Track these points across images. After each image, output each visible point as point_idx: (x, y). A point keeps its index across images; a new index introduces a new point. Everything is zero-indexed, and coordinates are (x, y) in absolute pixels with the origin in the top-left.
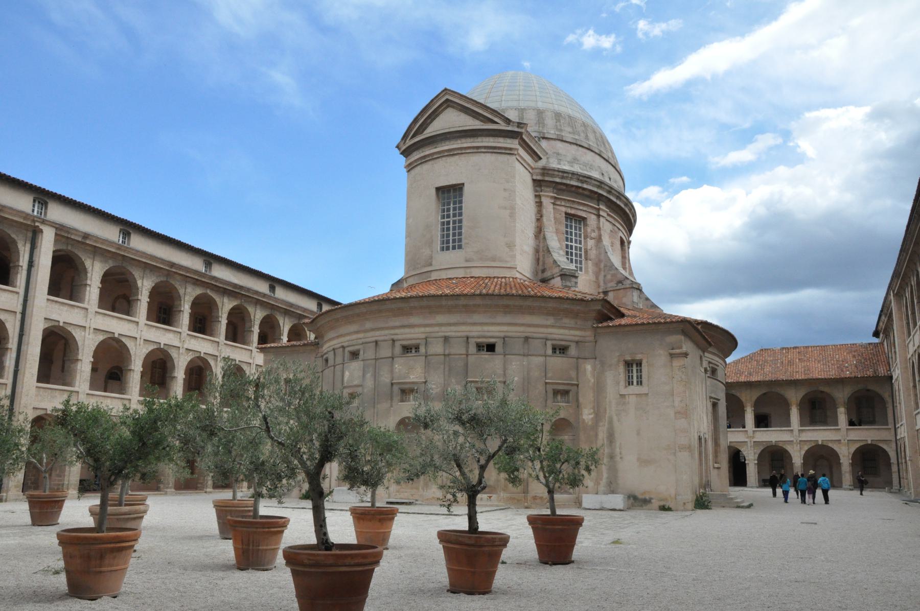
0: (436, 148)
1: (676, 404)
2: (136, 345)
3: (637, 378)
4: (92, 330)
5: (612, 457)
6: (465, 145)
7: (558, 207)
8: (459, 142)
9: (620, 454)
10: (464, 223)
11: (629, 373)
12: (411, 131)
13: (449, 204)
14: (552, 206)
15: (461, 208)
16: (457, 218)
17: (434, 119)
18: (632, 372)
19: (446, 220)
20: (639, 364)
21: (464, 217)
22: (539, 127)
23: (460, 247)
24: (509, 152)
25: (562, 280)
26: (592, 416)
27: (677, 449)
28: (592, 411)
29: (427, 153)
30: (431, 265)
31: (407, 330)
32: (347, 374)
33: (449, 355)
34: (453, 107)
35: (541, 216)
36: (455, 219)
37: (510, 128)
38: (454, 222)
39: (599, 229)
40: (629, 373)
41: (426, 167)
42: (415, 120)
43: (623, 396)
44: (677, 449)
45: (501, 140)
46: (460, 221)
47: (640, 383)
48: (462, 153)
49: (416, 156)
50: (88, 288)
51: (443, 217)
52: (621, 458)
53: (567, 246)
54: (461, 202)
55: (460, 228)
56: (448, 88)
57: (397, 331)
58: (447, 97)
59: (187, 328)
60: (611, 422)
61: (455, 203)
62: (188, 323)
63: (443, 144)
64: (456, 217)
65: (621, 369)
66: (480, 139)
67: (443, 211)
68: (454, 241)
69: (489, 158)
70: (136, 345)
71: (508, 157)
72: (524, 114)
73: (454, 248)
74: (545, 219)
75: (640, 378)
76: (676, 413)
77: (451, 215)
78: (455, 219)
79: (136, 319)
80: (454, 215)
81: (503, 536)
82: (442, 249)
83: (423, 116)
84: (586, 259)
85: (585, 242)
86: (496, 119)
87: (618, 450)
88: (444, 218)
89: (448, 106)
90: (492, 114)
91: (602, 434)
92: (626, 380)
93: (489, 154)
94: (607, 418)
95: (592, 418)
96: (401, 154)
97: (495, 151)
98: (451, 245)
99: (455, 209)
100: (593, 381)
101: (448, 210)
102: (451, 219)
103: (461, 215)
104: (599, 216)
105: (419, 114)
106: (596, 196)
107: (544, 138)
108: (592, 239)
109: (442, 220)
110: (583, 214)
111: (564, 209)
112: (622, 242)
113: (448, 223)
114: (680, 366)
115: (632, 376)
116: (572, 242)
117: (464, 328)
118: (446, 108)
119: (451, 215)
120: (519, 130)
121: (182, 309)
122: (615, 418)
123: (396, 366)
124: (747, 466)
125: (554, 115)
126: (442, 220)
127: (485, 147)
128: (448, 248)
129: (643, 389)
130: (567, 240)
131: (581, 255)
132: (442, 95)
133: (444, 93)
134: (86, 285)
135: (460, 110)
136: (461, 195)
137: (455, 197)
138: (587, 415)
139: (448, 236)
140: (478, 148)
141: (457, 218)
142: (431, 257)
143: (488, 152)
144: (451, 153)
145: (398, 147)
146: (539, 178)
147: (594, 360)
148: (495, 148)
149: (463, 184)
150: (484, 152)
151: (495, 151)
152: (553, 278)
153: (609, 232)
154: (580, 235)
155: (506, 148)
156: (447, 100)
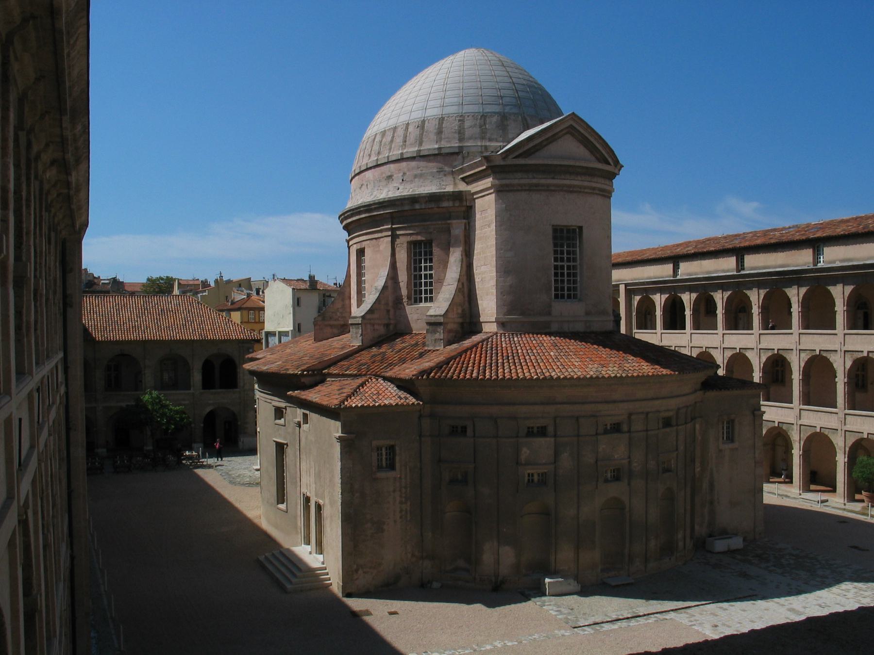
0: (553, 178)
1: (757, 455)
5: (712, 503)
6: (586, 184)
8: (579, 178)
17: (551, 142)
19: (559, 264)
23: (575, 296)
29: (543, 181)
30: (549, 313)
34: (573, 135)
36: (568, 264)
38: (569, 268)
43: (721, 451)
48: (580, 192)
51: (556, 260)
56: (576, 112)
63: (563, 177)
64: (570, 262)
66: (595, 179)
67: (556, 252)
73: (569, 297)
77: (565, 258)
78: (568, 264)
80: (569, 260)
82: (556, 296)
86: (610, 160)
88: (573, 266)
90: (608, 153)
99: (568, 253)
100: (700, 438)
102: (565, 264)
109: (556, 263)
113: (562, 267)
119: (565, 258)
126: (556, 263)
128: (563, 297)
129: (736, 445)
140: (594, 189)
143: (599, 194)
144: (571, 190)
149: (581, 228)
150: (597, 194)
156: (571, 125)
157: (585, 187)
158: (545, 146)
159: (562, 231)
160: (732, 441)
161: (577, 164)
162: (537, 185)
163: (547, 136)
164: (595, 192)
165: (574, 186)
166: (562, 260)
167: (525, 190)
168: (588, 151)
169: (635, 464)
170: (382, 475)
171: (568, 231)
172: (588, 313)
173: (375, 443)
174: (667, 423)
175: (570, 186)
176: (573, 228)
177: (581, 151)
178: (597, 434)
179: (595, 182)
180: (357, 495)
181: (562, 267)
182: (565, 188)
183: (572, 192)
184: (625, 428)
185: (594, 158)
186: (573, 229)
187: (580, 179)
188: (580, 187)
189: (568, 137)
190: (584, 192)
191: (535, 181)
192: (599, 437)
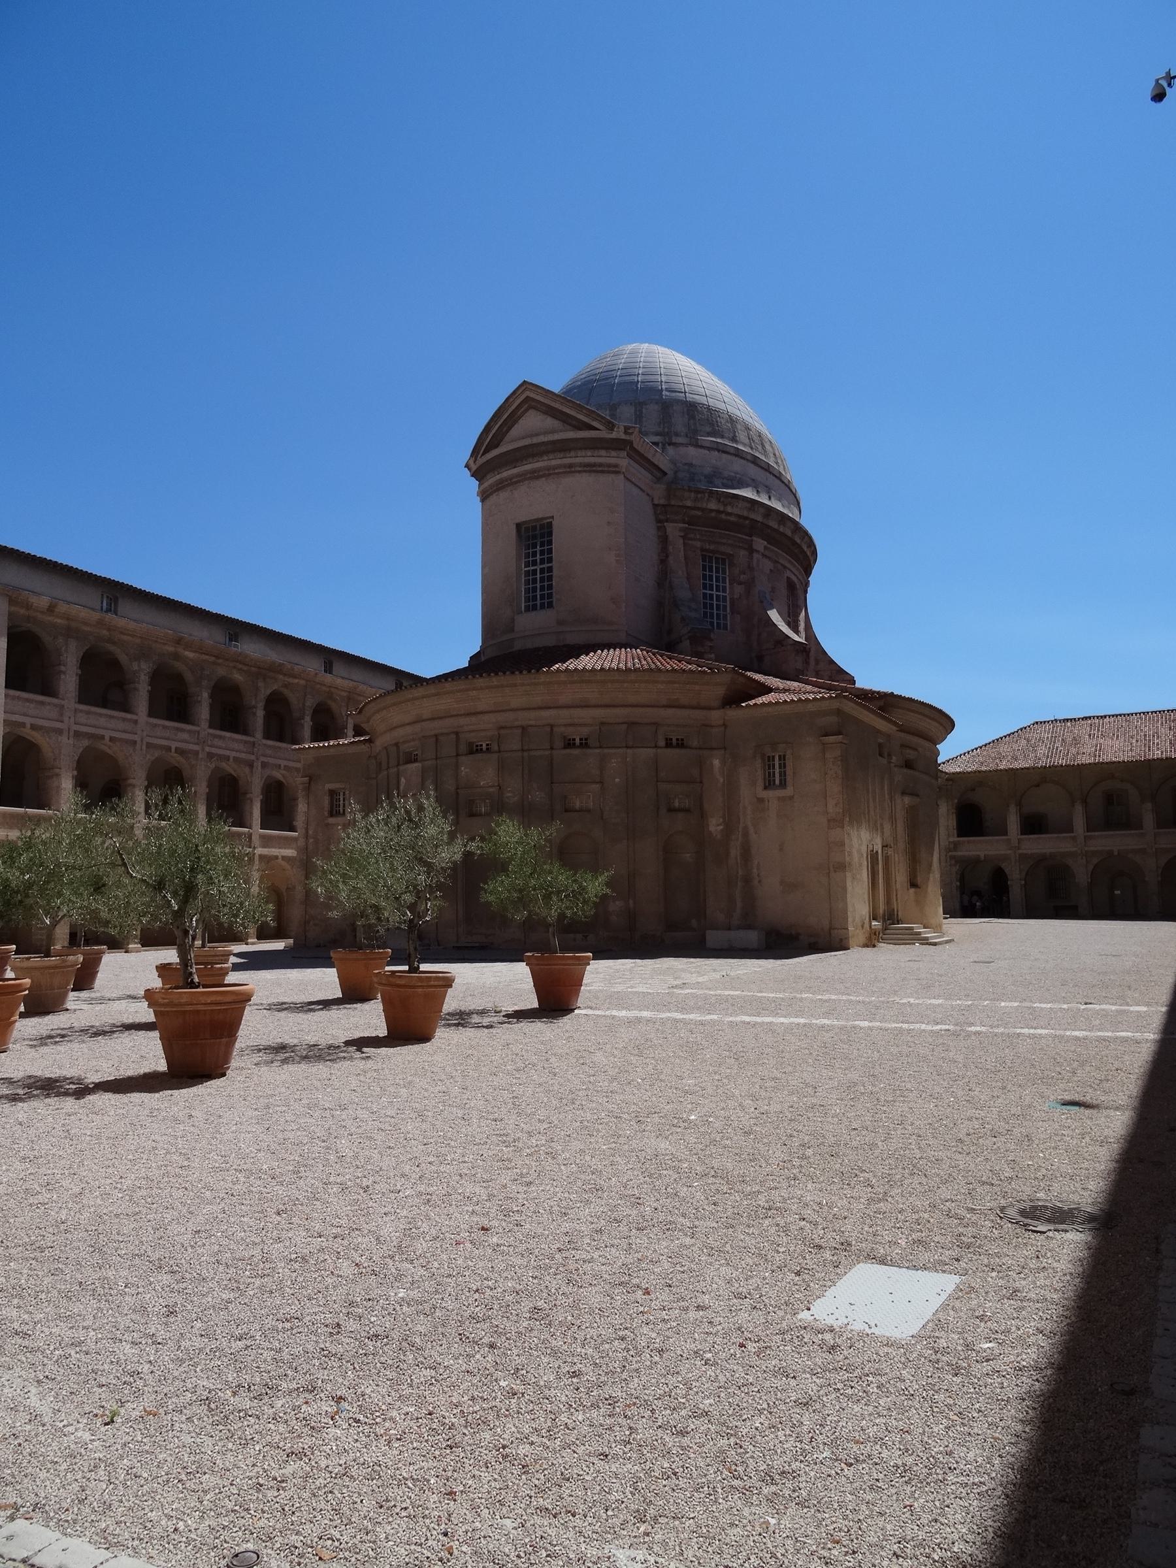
1: (831, 809)
2: (134, 750)
3: (780, 776)
4: (72, 733)
5: (747, 880)
6: (554, 463)
7: (690, 542)
9: (758, 875)
10: (555, 572)
11: (769, 768)
12: (483, 443)
13: (534, 546)
14: (681, 541)
15: (550, 551)
16: (546, 566)
18: (774, 768)
20: (783, 758)
21: (555, 564)
22: (664, 428)
23: (550, 605)
24: (613, 470)
25: (691, 644)
26: (721, 827)
27: (831, 869)
28: (721, 820)
30: (512, 630)
31: (474, 719)
32: (403, 780)
33: (529, 750)
35: (667, 556)
36: (542, 566)
37: (614, 435)
39: (751, 568)
40: (769, 768)
41: (503, 495)
42: (487, 428)
43: (761, 800)
44: (831, 869)
45: (603, 453)
46: (550, 569)
47: (783, 785)
48: (550, 475)
49: (491, 480)
50: (63, 677)
52: (760, 881)
53: (705, 594)
54: (550, 542)
55: (550, 578)
57: (463, 721)
58: (528, 393)
59: (207, 724)
60: (746, 834)
61: (542, 545)
62: (208, 717)
65: (758, 763)
66: (573, 454)
67: (527, 556)
68: (542, 597)
69: (586, 479)
70: (134, 750)
71: (613, 476)
72: (644, 410)
73: (542, 606)
74: (671, 558)
75: (783, 774)
76: (829, 821)
77: (538, 561)
78: (542, 566)
79: (134, 717)
81: (449, 975)
83: (496, 423)
84: (732, 612)
85: (730, 588)
86: (595, 424)
87: (755, 870)
89: (530, 407)
90: (588, 416)
91: (735, 852)
92: (765, 779)
93: (587, 474)
94: (740, 829)
95: (722, 830)
96: (472, 476)
97: (594, 469)
98: (538, 602)
99: (542, 552)
100: (722, 780)
101: (534, 554)
102: (538, 568)
103: (550, 560)
104: (751, 550)
105: (492, 419)
106: (747, 522)
107: (670, 444)
108: (740, 583)
110: (729, 551)
111: (698, 544)
112: (791, 586)
113: (534, 572)
114: (835, 758)
115: (774, 773)
116: (713, 590)
117: (546, 714)
118: (526, 410)
119: (538, 561)
120: (627, 437)
121: (199, 698)
122: (751, 830)
123: (463, 768)
124: (1010, 889)
125: (685, 410)
127: (581, 465)
128: (534, 608)
129: (788, 791)
130: (705, 587)
131: (725, 607)
132: (521, 391)
133: (523, 388)
134: (61, 672)
135: (545, 413)
136: (550, 534)
137: (542, 536)
138: (715, 826)
139: (534, 590)
140: (571, 466)
141: (546, 566)
142: (513, 620)
143: (585, 471)
144: (535, 475)
145: (467, 466)
146: (662, 502)
147: (723, 752)
148: (594, 465)
150: (579, 472)
151: (594, 469)
152: (681, 642)
153: (768, 572)
154: (724, 579)
155: (609, 466)
156: (527, 397)
157: (555, 468)
158: (507, 432)
159: (534, 528)
160: (783, 785)
161: (535, 440)
162: (501, 481)
163: (502, 420)
164: (573, 469)
165: (540, 469)
166: (534, 563)
167: (495, 491)
168: (558, 422)
169: (509, 795)
170: (331, 820)
171: (542, 527)
172: (560, 623)
173: (329, 786)
174: (569, 744)
175: (533, 471)
176: (548, 520)
177: (550, 422)
178: (458, 755)
179: (571, 457)
180: (311, 840)
181: (534, 572)
182: (529, 475)
183: (537, 478)
184: (495, 748)
185: (569, 427)
186: (548, 523)
187: (546, 458)
188: (548, 468)
189: (532, 413)
190: (556, 473)
191: (498, 477)
192: (462, 759)
